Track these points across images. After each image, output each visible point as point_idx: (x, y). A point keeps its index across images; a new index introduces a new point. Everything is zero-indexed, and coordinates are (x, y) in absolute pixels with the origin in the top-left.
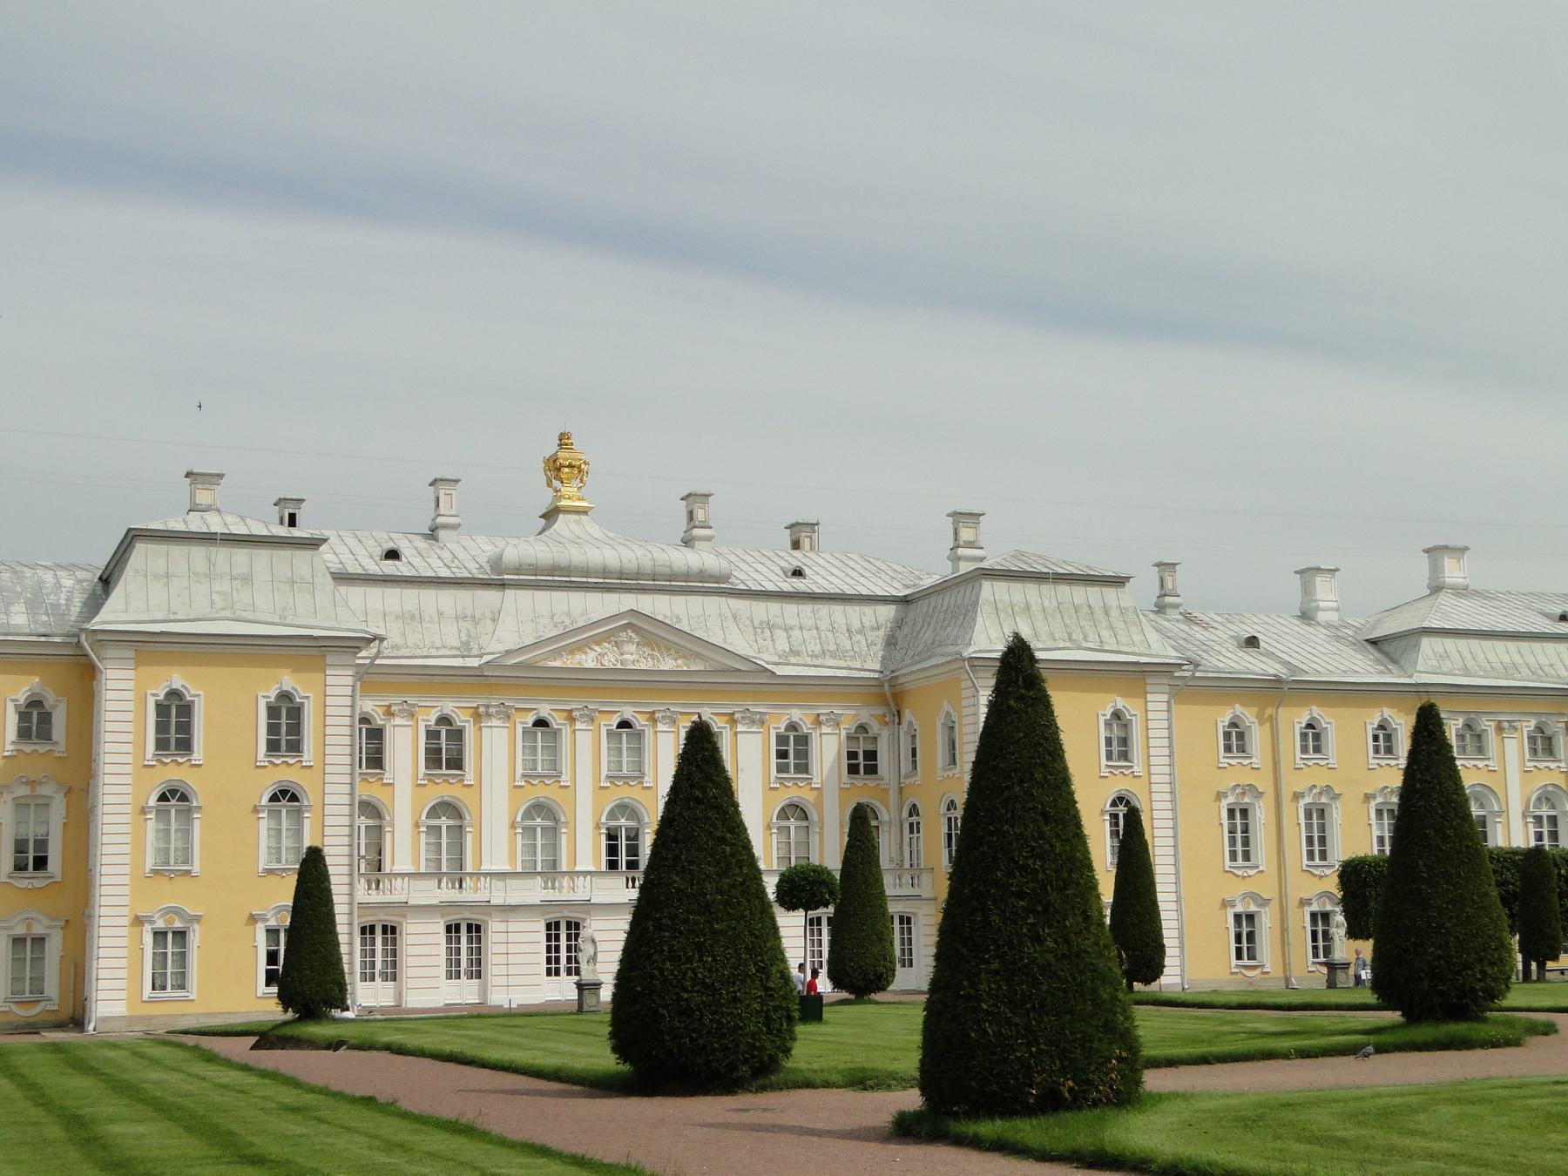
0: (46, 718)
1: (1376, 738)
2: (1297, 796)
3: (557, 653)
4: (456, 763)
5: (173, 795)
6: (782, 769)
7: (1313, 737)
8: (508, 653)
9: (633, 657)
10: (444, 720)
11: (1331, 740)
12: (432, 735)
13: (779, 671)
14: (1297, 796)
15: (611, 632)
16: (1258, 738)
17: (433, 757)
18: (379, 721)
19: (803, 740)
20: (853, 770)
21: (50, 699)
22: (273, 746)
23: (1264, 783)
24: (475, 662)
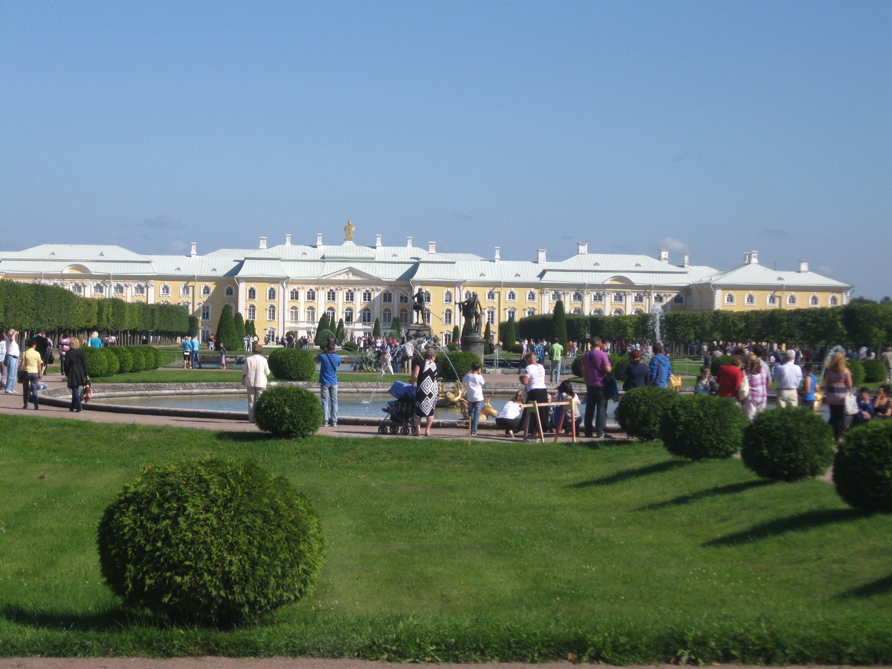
0: (232, 291)
1: (529, 295)
2: (505, 309)
3: (334, 276)
4: (313, 298)
5: (252, 306)
6: (385, 300)
7: (512, 296)
8: (324, 276)
9: (352, 277)
10: (311, 290)
11: (517, 297)
12: (309, 293)
13: (383, 280)
14: (505, 309)
15: (347, 272)
16: (496, 296)
17: (309, 298)
18: (297, 290)
19: (390, 294)
20: (401, 300)
21: (232, 287)
22: (270, 298)
23: (496, 306)
24: (316, 278)
